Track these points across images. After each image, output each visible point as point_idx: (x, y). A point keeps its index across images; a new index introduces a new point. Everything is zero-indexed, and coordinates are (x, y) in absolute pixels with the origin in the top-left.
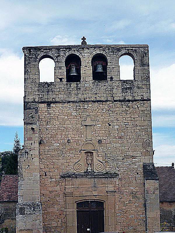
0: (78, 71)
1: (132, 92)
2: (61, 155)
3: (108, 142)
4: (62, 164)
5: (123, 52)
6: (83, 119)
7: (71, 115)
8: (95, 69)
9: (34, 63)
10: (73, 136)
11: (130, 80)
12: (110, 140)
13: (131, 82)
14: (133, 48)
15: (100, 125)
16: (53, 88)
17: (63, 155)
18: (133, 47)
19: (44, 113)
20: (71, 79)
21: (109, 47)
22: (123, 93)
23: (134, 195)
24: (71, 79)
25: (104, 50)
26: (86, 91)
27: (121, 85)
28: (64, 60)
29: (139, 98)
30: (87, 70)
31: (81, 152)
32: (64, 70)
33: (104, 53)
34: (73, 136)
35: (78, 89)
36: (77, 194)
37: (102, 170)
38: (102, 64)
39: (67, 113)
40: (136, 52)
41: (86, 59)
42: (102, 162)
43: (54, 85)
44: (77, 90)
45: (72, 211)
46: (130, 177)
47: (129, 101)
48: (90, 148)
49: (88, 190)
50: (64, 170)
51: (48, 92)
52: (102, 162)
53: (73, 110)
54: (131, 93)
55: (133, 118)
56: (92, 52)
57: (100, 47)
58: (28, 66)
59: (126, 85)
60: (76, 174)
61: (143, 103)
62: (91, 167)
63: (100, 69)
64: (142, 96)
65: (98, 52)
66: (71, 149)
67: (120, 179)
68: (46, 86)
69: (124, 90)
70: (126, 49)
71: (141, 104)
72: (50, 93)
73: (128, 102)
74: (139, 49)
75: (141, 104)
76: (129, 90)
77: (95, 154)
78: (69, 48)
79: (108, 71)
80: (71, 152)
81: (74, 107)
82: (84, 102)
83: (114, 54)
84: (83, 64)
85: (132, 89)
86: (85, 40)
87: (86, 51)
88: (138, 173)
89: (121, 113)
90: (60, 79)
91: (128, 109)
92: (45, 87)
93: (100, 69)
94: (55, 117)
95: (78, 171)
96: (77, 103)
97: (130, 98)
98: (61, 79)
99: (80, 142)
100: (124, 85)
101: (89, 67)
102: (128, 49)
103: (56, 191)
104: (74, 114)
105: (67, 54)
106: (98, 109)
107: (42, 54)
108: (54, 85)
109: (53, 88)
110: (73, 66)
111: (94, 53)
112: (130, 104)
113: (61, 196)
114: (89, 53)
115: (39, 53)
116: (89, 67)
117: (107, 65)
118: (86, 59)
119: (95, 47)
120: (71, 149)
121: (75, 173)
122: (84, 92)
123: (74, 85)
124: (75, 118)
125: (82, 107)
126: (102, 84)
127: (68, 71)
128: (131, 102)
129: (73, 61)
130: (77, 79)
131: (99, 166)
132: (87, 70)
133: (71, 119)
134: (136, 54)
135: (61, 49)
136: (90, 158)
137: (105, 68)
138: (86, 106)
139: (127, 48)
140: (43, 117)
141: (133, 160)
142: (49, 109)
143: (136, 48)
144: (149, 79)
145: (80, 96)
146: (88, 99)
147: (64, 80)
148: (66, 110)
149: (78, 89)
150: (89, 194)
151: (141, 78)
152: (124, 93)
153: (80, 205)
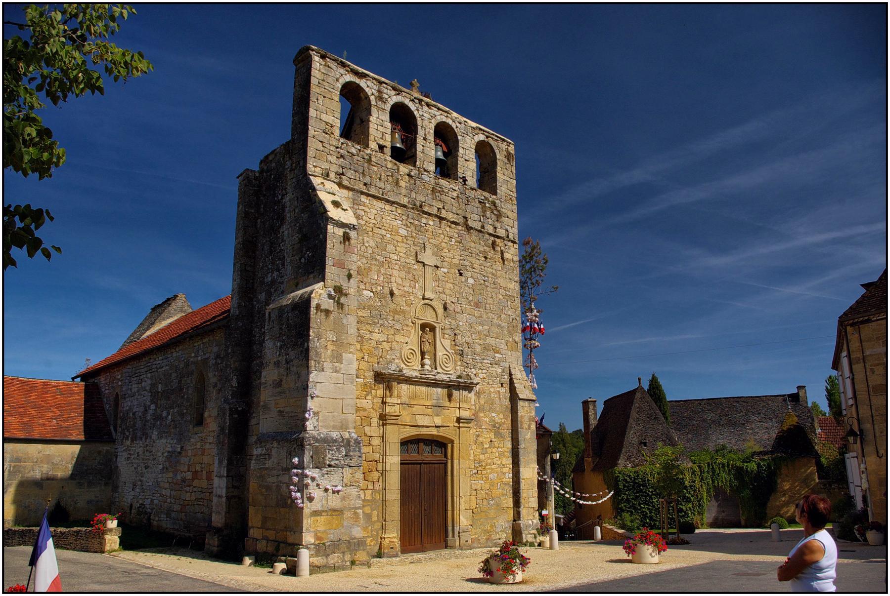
4: (378, 343)
5: (482, 137)
10: (400, 281)
15: (446, 270)
23: (495, 427)
33: (454, 126)
34: (400, 281)
36: (406, 418)
45: (394, 460)
46: (492, 390)
49: (422, 412)
65: (444, 119)
67: (478, 394)
80: (397, 317)
84: (421, 132)
88: (502, 386)
94: (368, 229)
99: (412, 298)
103: (365, 410)
104: (403, 232)
107: (349, 78)
113: (375, 421)
115: (342, 71)
123: (404, 169)
138: (424, 221)
141: (497, 355)
142: (356, 207)
147: (388, 151)
150: (426, 421)
153: (406, 443)
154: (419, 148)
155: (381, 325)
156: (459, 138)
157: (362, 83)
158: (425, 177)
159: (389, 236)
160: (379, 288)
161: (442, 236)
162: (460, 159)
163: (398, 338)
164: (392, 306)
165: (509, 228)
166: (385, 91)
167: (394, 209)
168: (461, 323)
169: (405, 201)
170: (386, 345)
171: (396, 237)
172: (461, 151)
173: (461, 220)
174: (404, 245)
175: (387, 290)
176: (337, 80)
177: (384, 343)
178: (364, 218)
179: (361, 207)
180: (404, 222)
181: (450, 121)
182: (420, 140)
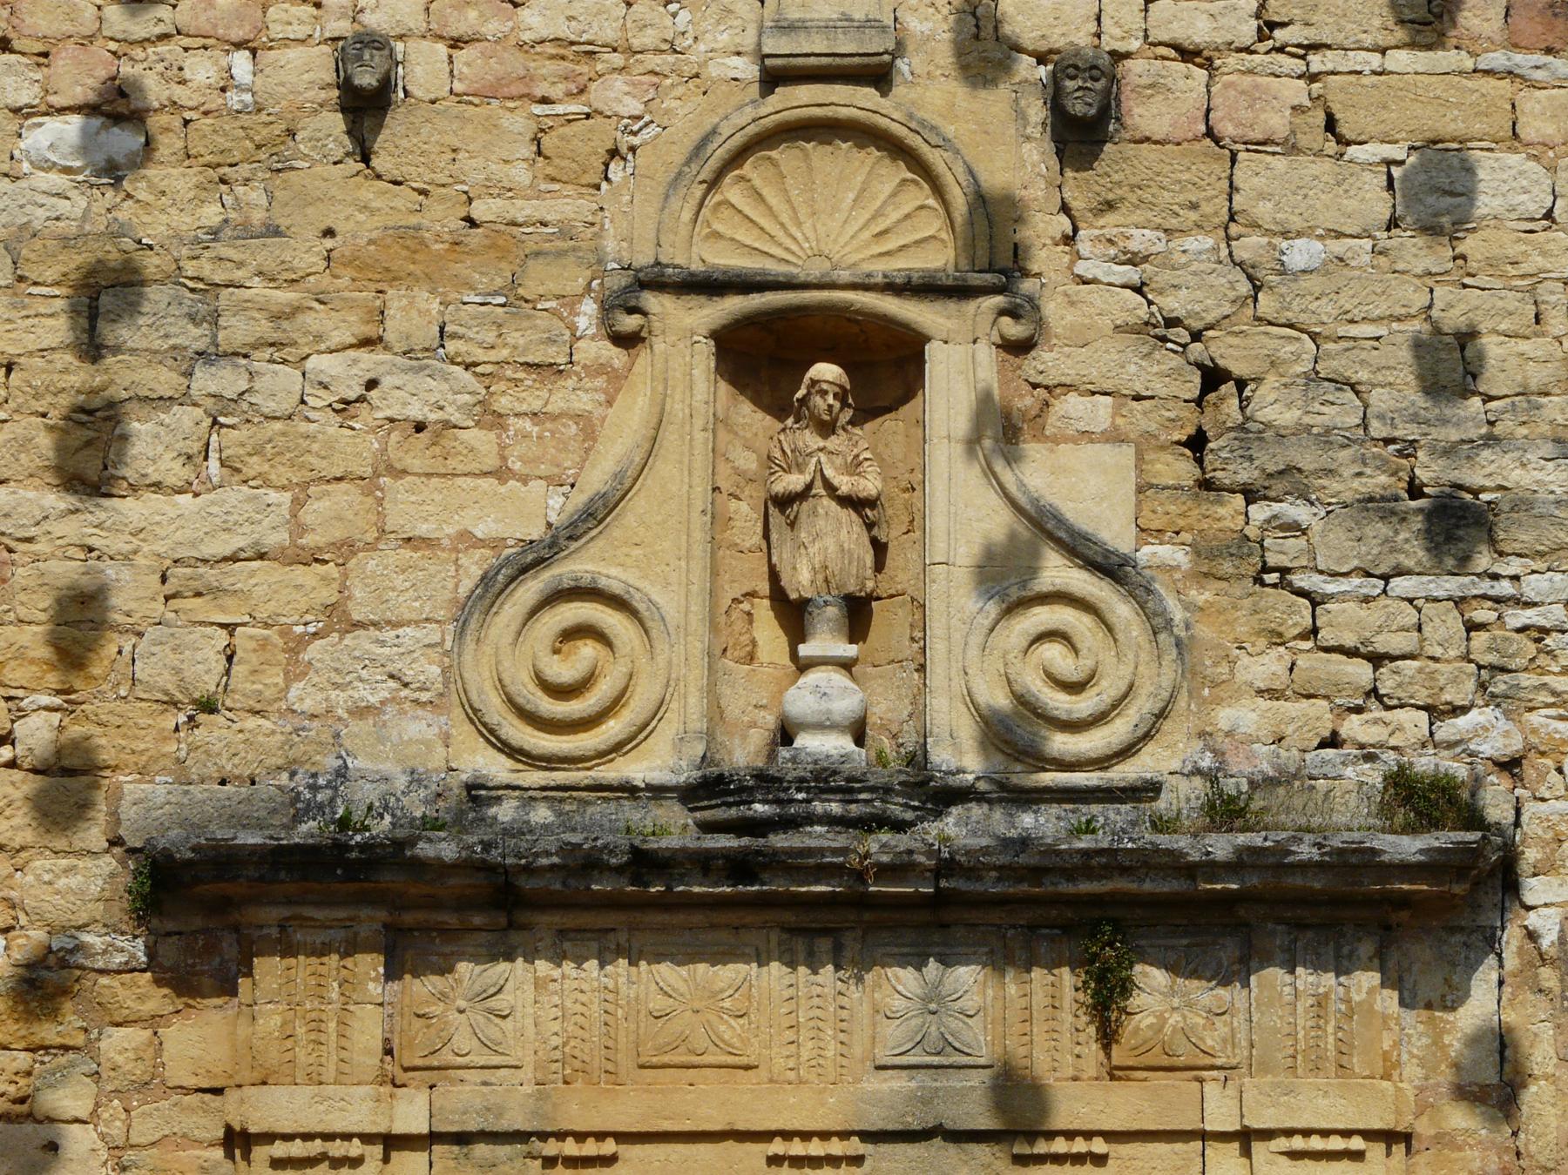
2: (164, 380)
3: (1277, 122)
4: (179, 581)
12: (1317, 62)
17: (207, 380)
31: (630, 323)
37: (1126, 752)
42: (1111, 568)
48: (839, 227)
50: (213, 730)
52: (1111, 568)
60: (505, 812)
62: (847, 665)
66: (396, 260)
77: (960, 362)
80: (412, 313)
95: (550, 762)
120: (396, 260)
121: (478, 793)
131: (1053, 652)
136: (855, 467)
155: (219, 414)
160: (202, 70)
163: (409, 506)
164: (361, 209)
168: (1301, 253)
170: (290, 593)
175: (304, 72)
177: (258, 578)
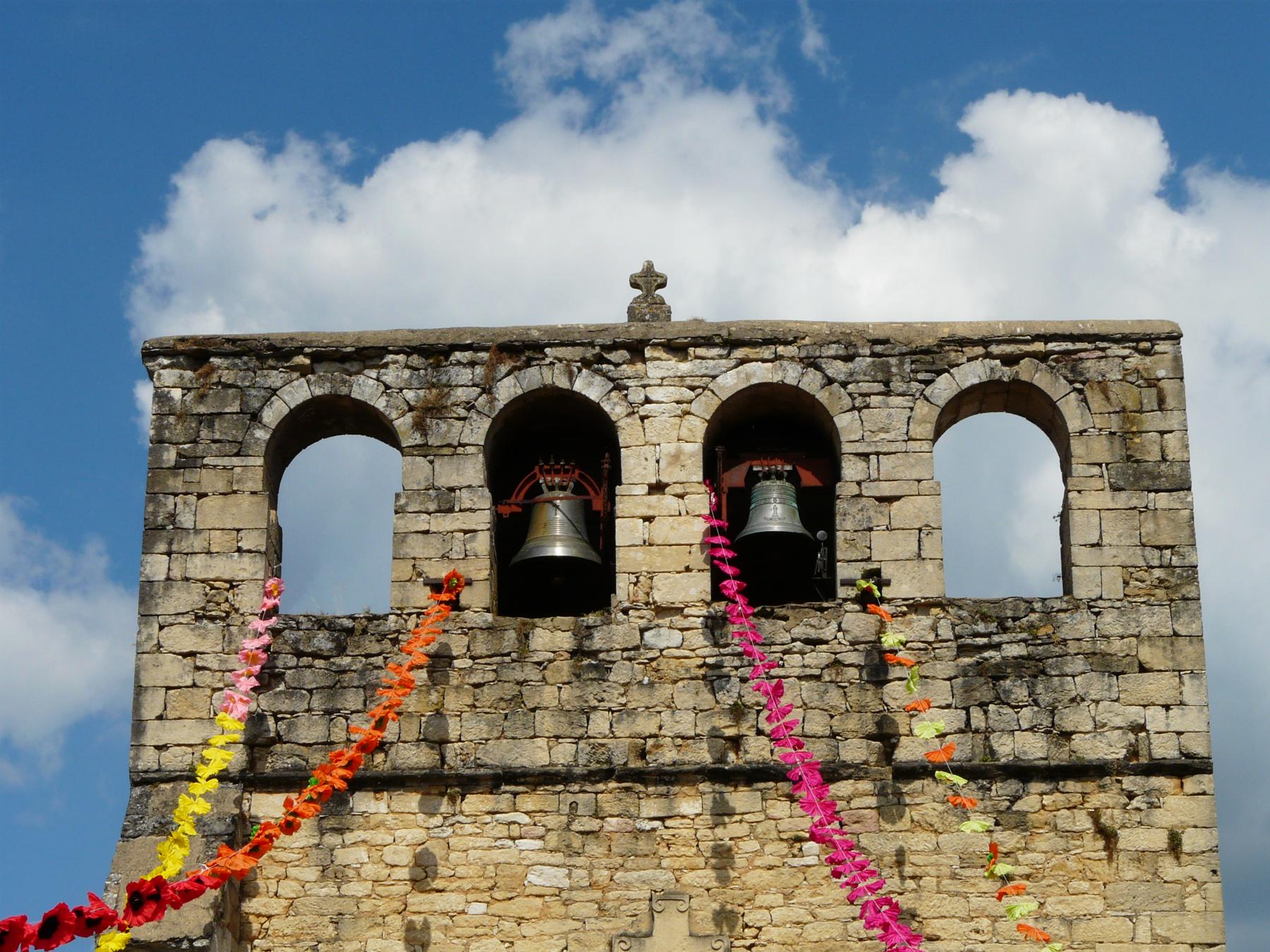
0: (598, 528)
1: (1045, 699)
5: (972, 373)
6: (623, 924)
7: (518, 889)
8: (732, 510)
9: (226, 461)
11: (1029, 602)
13: (1033, 617)
14: (1052, 346)
16: (379, 661)
18: (1046, 338)
19: (293, 872)
20: (530, 588)
21: (848, 342)
22: (967, 709)
24: (530, 588)
25: (811, 363)
26: (651, 684)
27: (957, 637)
28: (477, 431)
29: (1111, 748)
30: (663, 530)
32: (478, 514)
33: (811, 382)
35: (588, 661)
38: (793, 478)
39: (485, 866)
40: (1073, 370)
41: (661, 440)
43: (383, 636)
44: (578, 676)
47: (1023, 772)
51: (334, 688)
53: (539, 844)
54: (1036, 703)
55: (1063, 918)
56: (714, 377)
57: (771, 339)
58: (176, 483)
59: (996, 639)
61: (1147, 793)
63: (775, 514)
64: (1131, 736)
65: (760, 373)
68: (322, 641)
69: (985, 679)
70: (988, 355)
71: (1131, 796)
72: (352, 700)
73: (1013, 786)
74: (1103, 350)
75: (1131, 796)
76: (1021, 677)
78: (520, 349)
79: (847, 521)
81: (551, 821)
82: (640, 777)
83: (887, 393)
84: (636, 467)
85: (1043, 672)
86: (659, 292)
87: (661, 366)
89: (954, 876)
90: (436, 587)
91: (1009, 840)
92: (315, 655)
93: (775, 514)
96: (576, 788)
97: (1034, 748)
98: (448, 591)
100: (981, 641)
101: (681, 496)
102: (1008, 349)
104: (547, 877)
105: (507, 390)
106: (752, 834)
107: (298, 392)
108: (383, 636)
109: (379, 661)
110: (551, 488)
111: (731, 382)
112: (1034, 799)
114: (688, 381)
115: (275, 378)
116: (681, 496)
117: (838, 478)
118: (661, 440)
119: (731, 342)
122: (637, 698)
123: (552, 637)
124: (557, 908)
125: (614, 820)
126: (790, 628)
127: (511, 533)
128: (1036, 787)
129: (553, 440)
130: (584, 586)
132: (663, 530)
133: (520, 921)
134: (1080, 391)
135: (458, 355)
137: (818, 507)
139: (999, 342)
140: (276, 906)
143: (1079, 345)
144: (1188, 591)
145: (600, 724)
146: (668, 756)
147: (478, 597)
148: (480, 842)
149: (588, 661)
151: (1126, 583)
152: (983, 705)
154: (626, 531)
156: (843, 421)
157: (365, 388)
158: (664, 637)
159: (482, 908)
161: (753, 845)
162: (841, 506)
165: (1155, 719)
166: (466, 375)
167: (504, 801)
169: (563, 754)
171: (519, 906)
172: (851, 470)
173: (855, 751)
174: (549, 926)
176: (255, 417)
178: (369, 870)
179: (349, 837)
180: (553, 840)
181: (791, 374)
182: (631, 501)
